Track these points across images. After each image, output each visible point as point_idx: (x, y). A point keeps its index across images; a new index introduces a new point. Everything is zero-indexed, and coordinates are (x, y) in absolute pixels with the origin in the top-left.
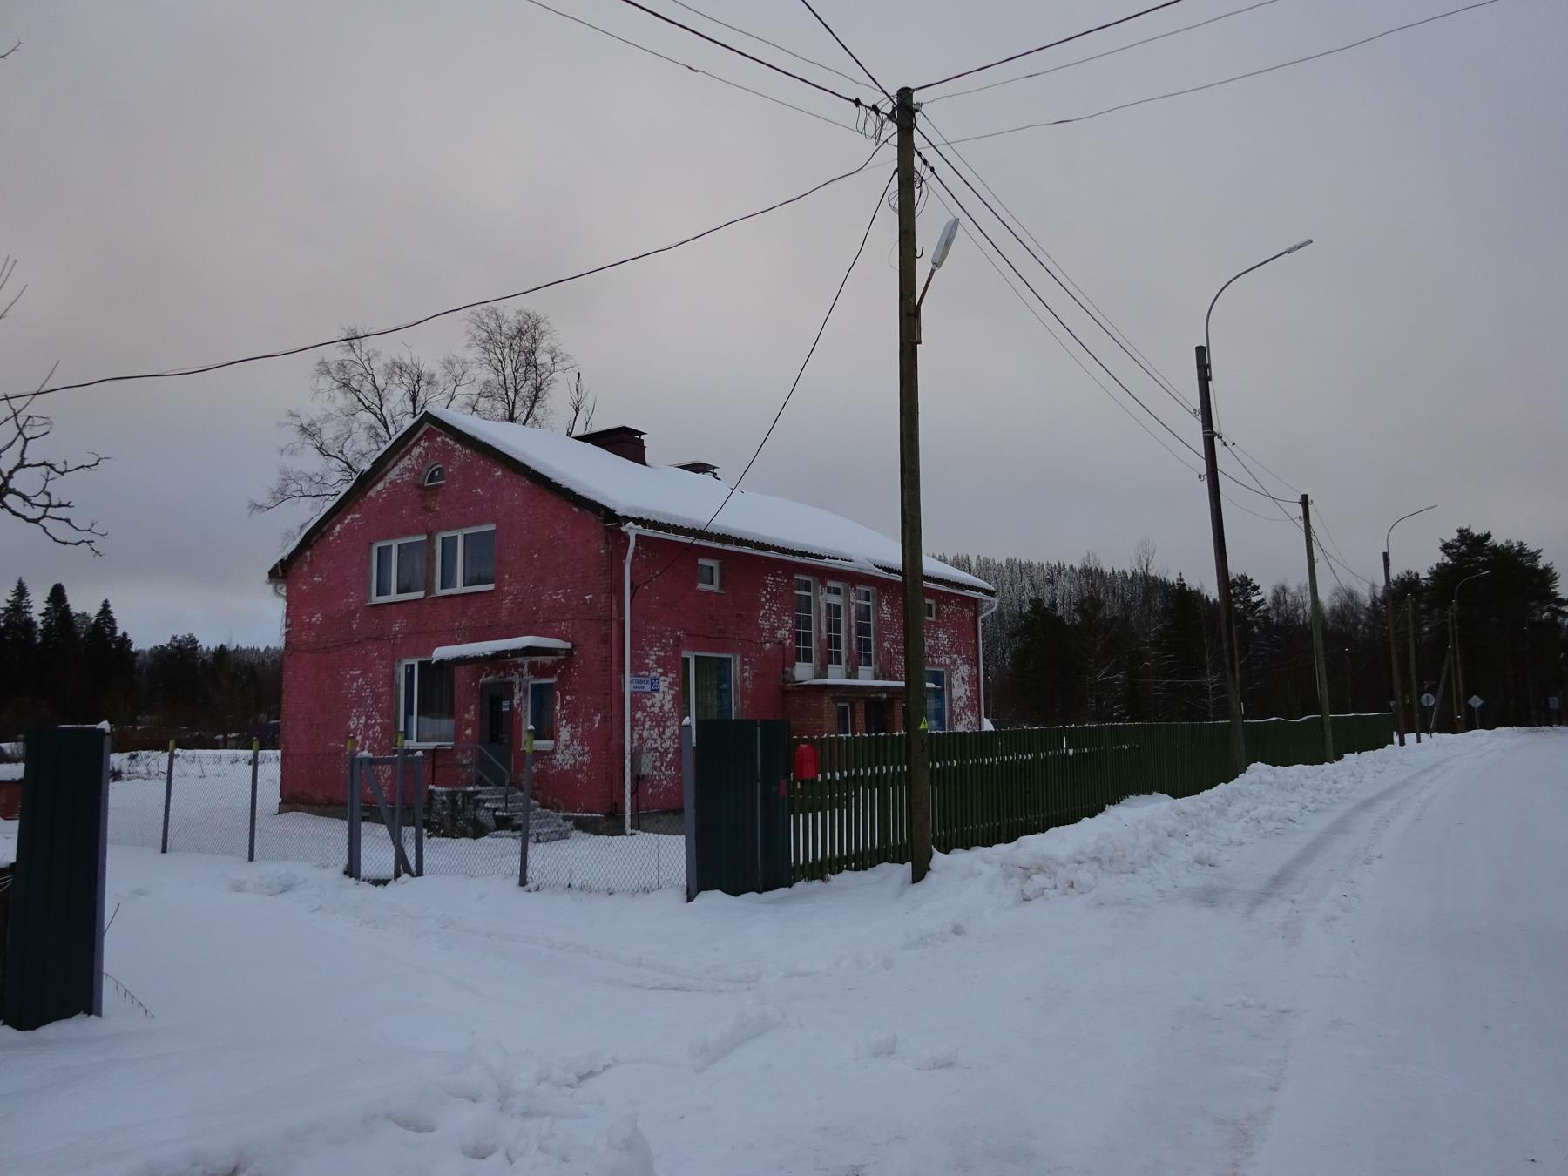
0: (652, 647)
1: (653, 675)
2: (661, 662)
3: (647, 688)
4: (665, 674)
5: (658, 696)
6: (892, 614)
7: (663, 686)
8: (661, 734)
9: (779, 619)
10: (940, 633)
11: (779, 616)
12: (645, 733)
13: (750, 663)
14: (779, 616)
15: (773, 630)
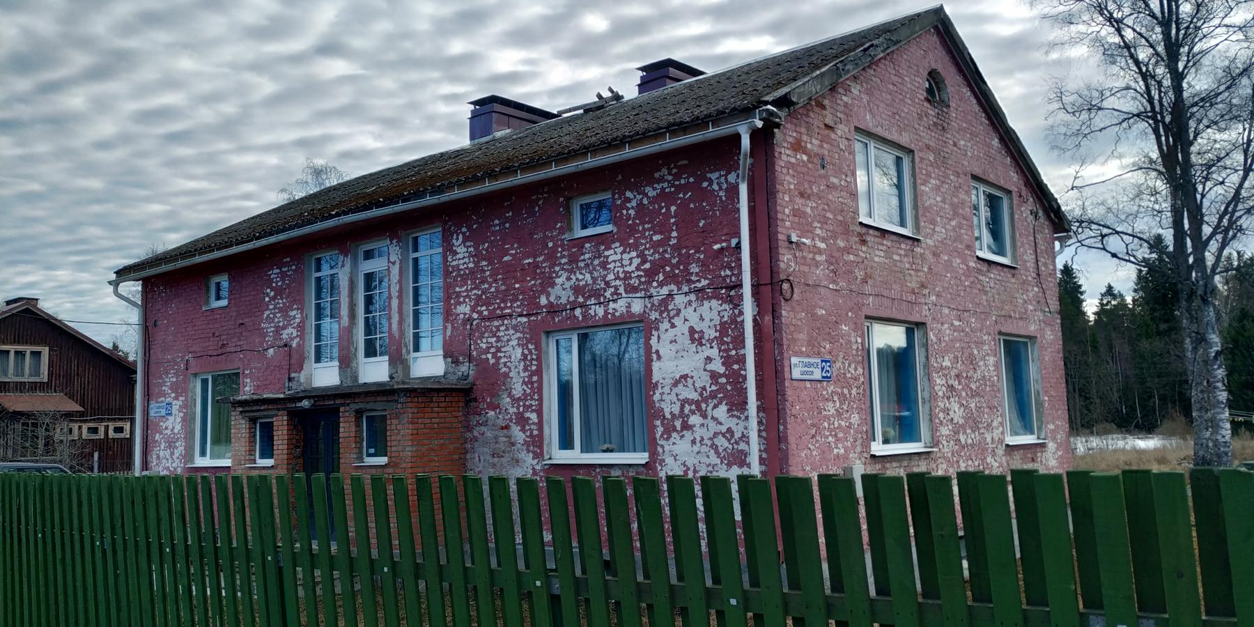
0: (167, 373)
1: (168, 400)
2: (174, 388)
3: (163, 412)
4: (176, 398)
5: (171, 419)
6: (477, 256)
7: (175, 409)
8: (172, 454)
9: (286, 316)
10: (614, 254)
11: (284, 311)
12: (162, 454)
13: (251, 376)
14: (284, 311)
15: (278, 330)
